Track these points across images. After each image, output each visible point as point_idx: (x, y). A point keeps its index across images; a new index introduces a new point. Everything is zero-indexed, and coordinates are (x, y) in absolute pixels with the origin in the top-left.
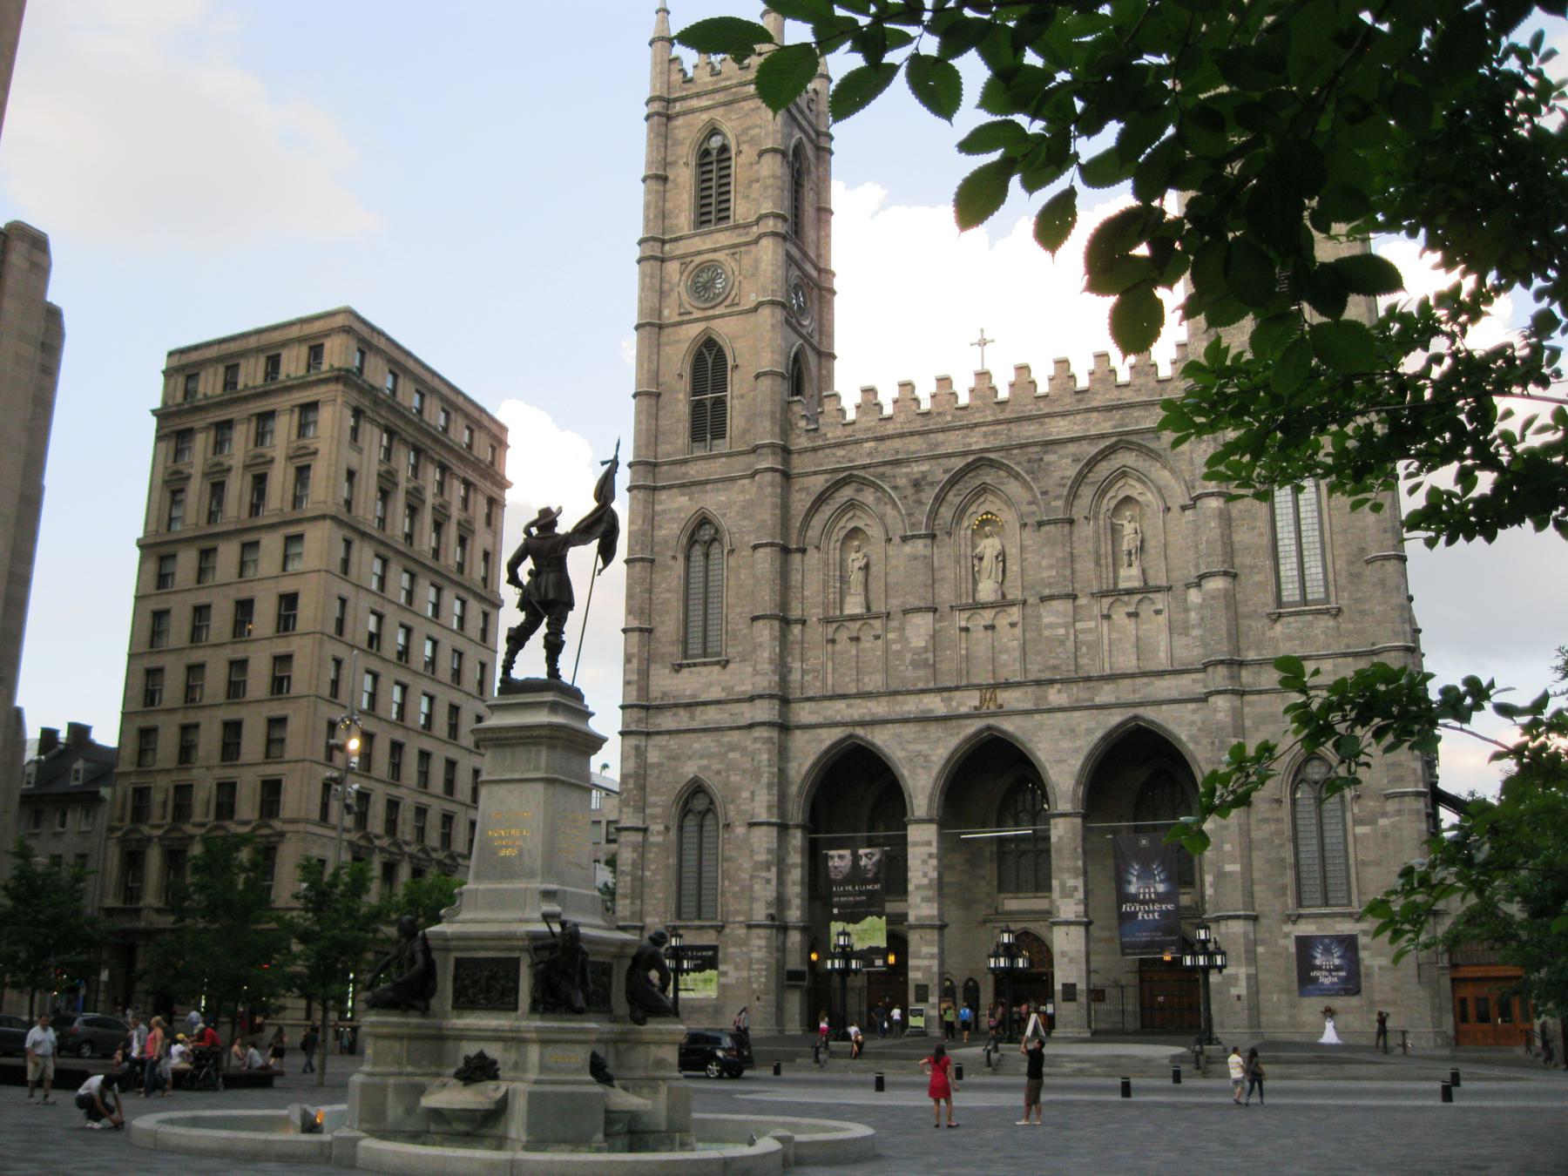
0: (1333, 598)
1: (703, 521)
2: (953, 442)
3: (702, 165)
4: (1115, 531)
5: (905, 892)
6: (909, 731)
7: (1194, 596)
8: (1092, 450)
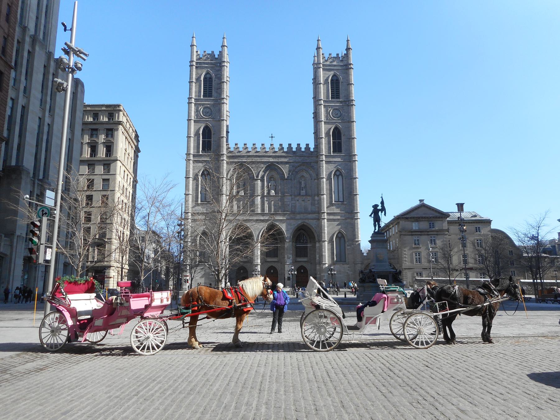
2: (265, 160)
4: (300, 183)
8: (297, 165)
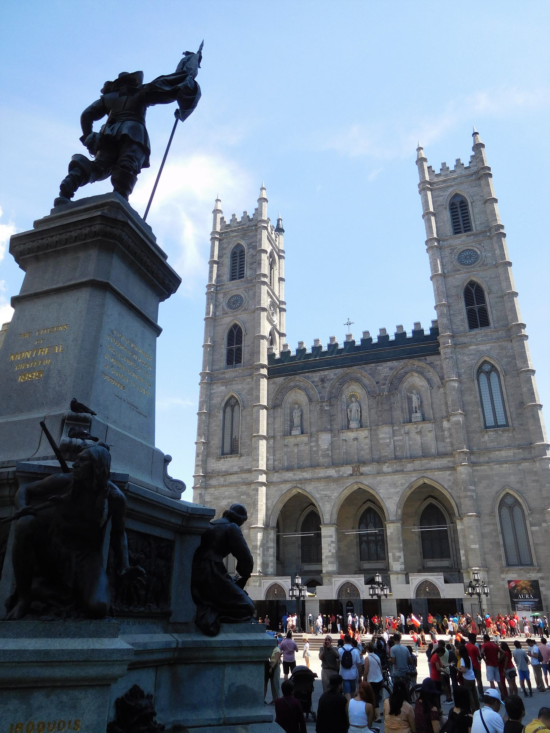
0: (510, 424)
1: (232, 397)
3: (234, 257)
4: (410, 400)
5: (319, 560)
6: (321, 485)
7: (445, 424)
